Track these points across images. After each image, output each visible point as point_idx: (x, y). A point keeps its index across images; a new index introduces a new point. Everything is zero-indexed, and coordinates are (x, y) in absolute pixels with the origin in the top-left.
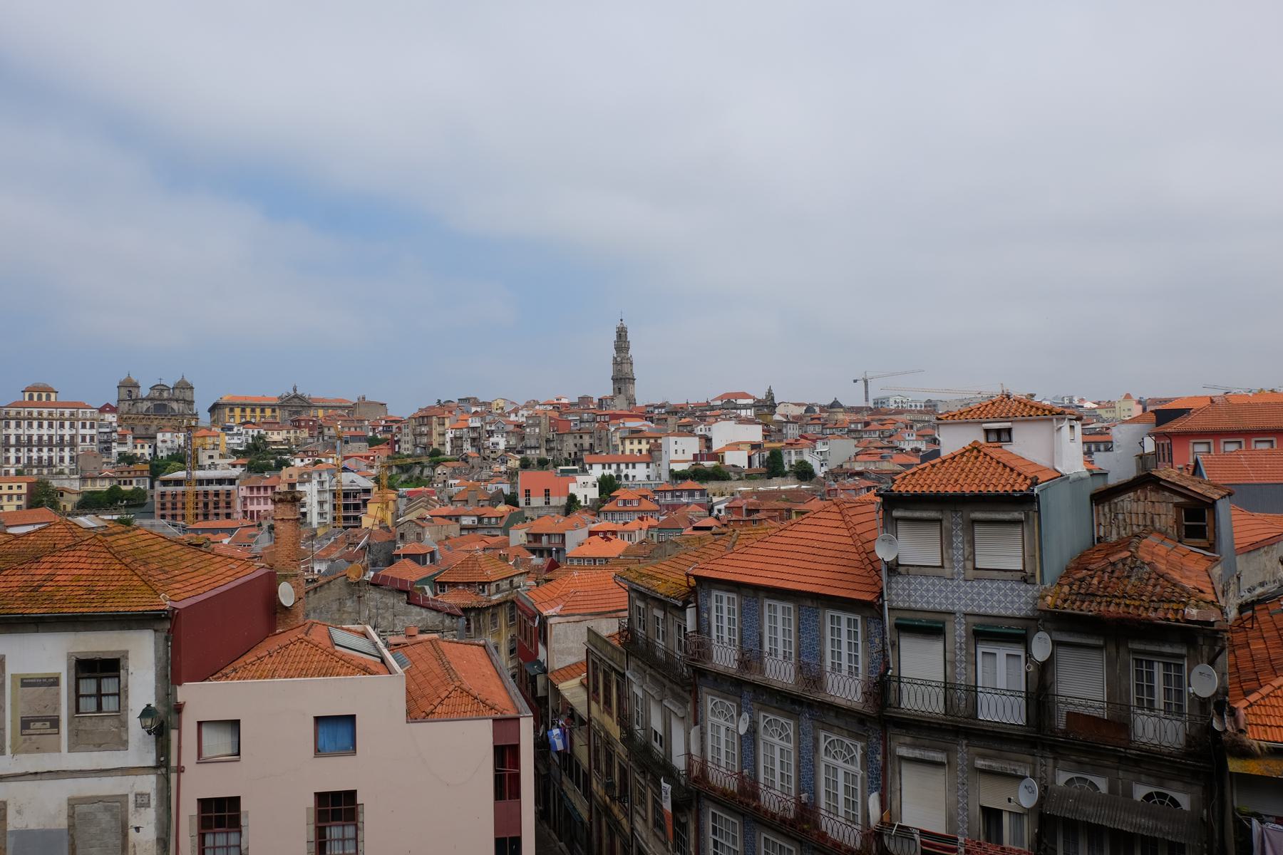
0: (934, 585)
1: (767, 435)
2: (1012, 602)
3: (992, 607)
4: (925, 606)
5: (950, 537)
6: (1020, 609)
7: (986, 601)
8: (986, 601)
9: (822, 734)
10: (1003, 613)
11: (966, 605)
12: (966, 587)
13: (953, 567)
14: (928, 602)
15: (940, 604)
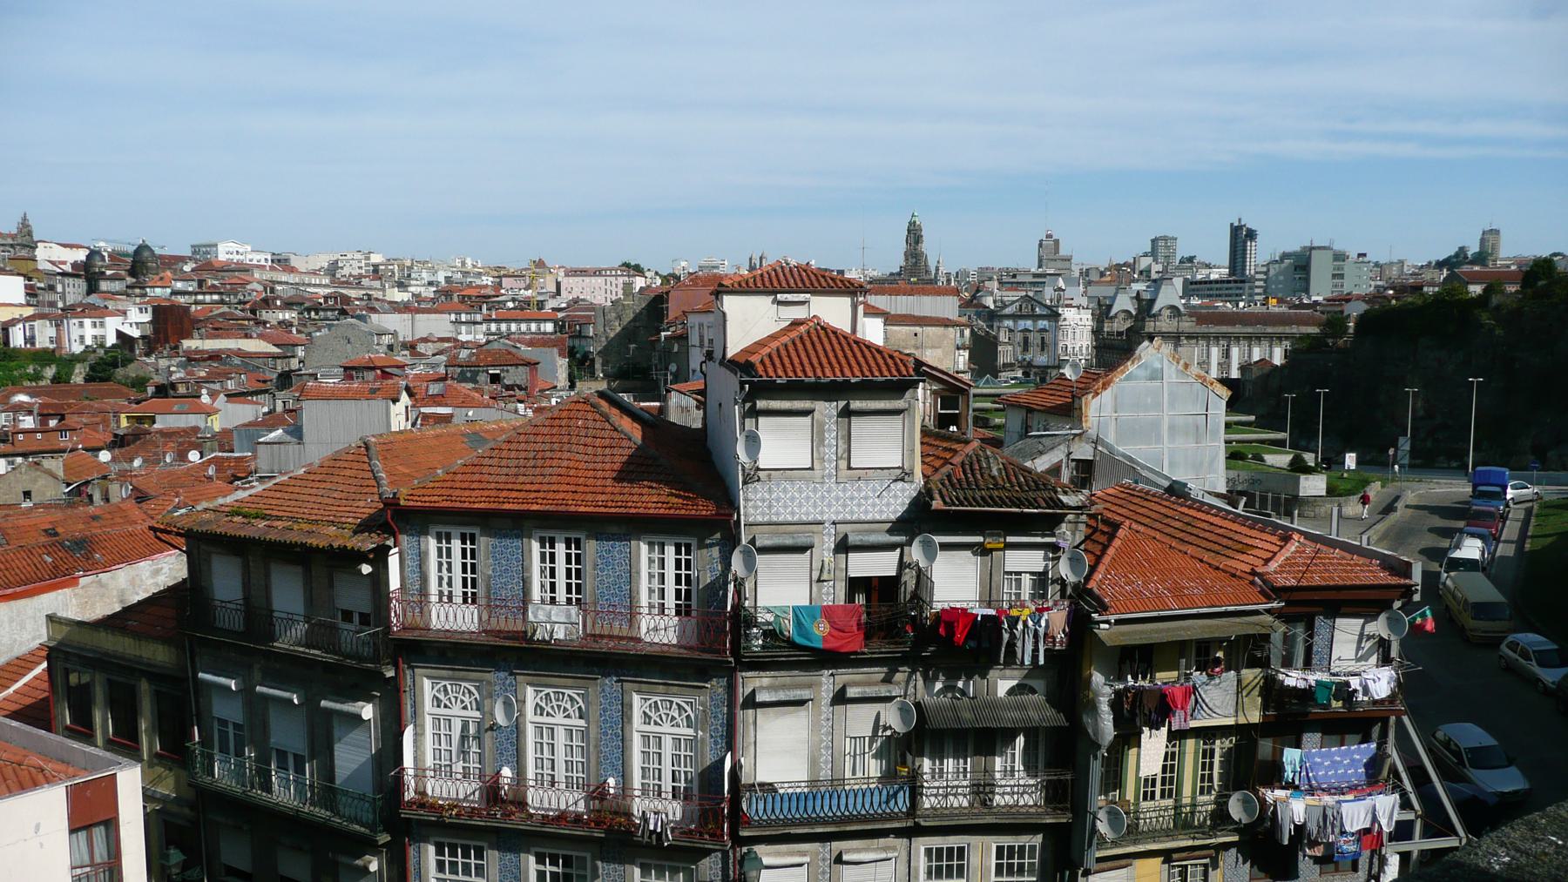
0: (800, 491)
1: (31, 292)
2: (888, 505)
3: (866, 512)
4: (790, 519)
5: (822, 432)
6: (895, 512)
7: (859, 505)
8: (859, 505)
9: (636, 698)
10: (878, 517)
11: (838, 513)
12: (837, 491)
13: (824, 469)
14: (793, 513)
15: (807, 514)
